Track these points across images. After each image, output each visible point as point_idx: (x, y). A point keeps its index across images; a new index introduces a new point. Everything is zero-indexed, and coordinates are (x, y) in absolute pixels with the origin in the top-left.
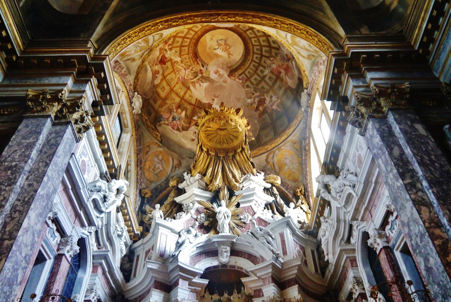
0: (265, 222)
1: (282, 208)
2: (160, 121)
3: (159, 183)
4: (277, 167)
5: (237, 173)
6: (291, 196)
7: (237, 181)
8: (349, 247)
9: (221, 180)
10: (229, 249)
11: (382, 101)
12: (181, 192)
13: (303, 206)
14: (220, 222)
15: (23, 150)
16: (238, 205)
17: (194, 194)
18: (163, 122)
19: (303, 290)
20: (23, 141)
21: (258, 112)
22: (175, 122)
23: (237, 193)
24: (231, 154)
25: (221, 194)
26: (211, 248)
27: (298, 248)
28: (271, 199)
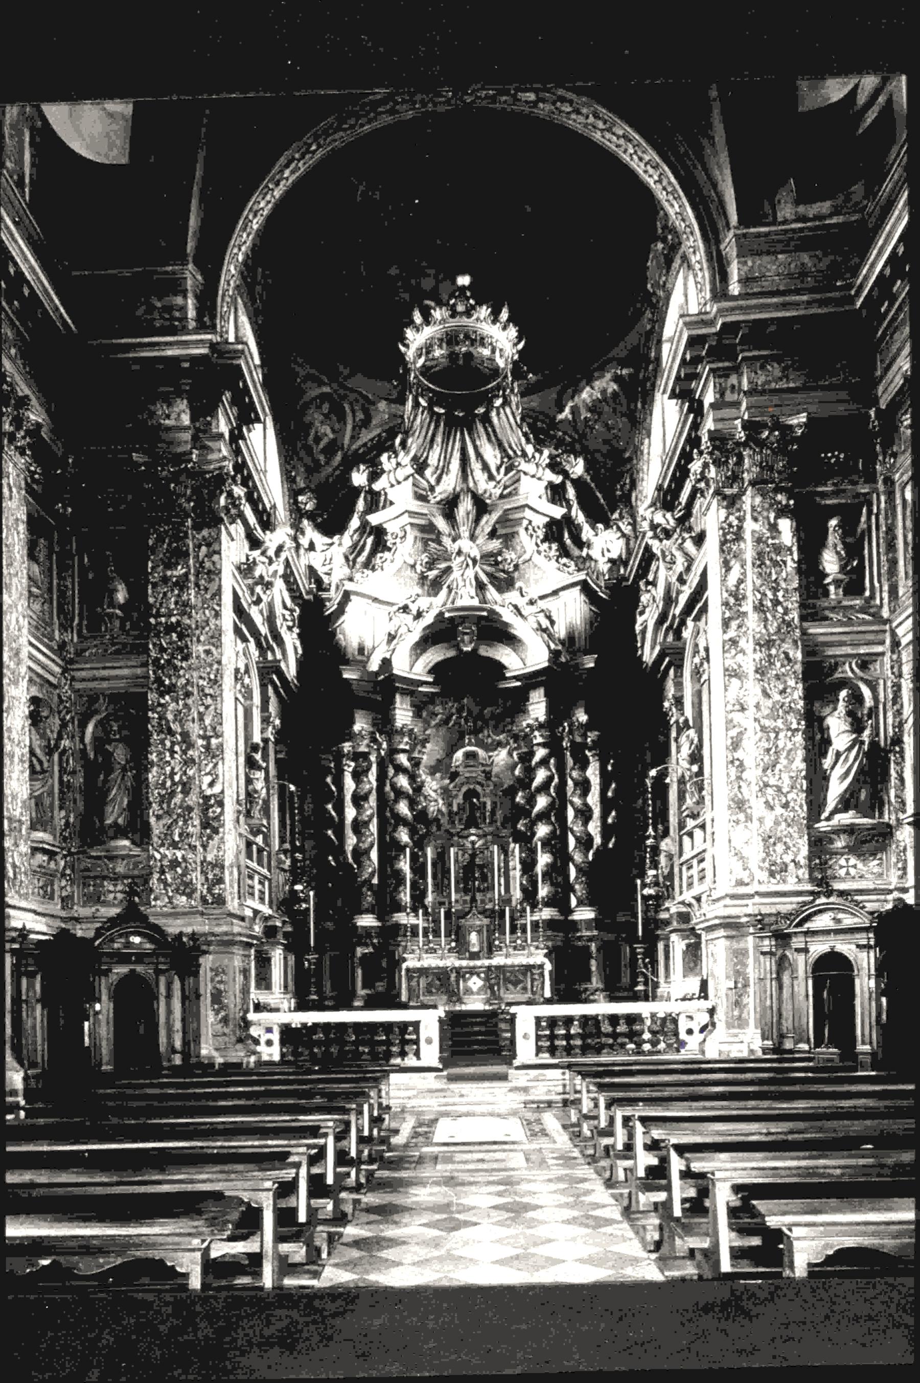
15: (176, 592)
20: (169, 573)
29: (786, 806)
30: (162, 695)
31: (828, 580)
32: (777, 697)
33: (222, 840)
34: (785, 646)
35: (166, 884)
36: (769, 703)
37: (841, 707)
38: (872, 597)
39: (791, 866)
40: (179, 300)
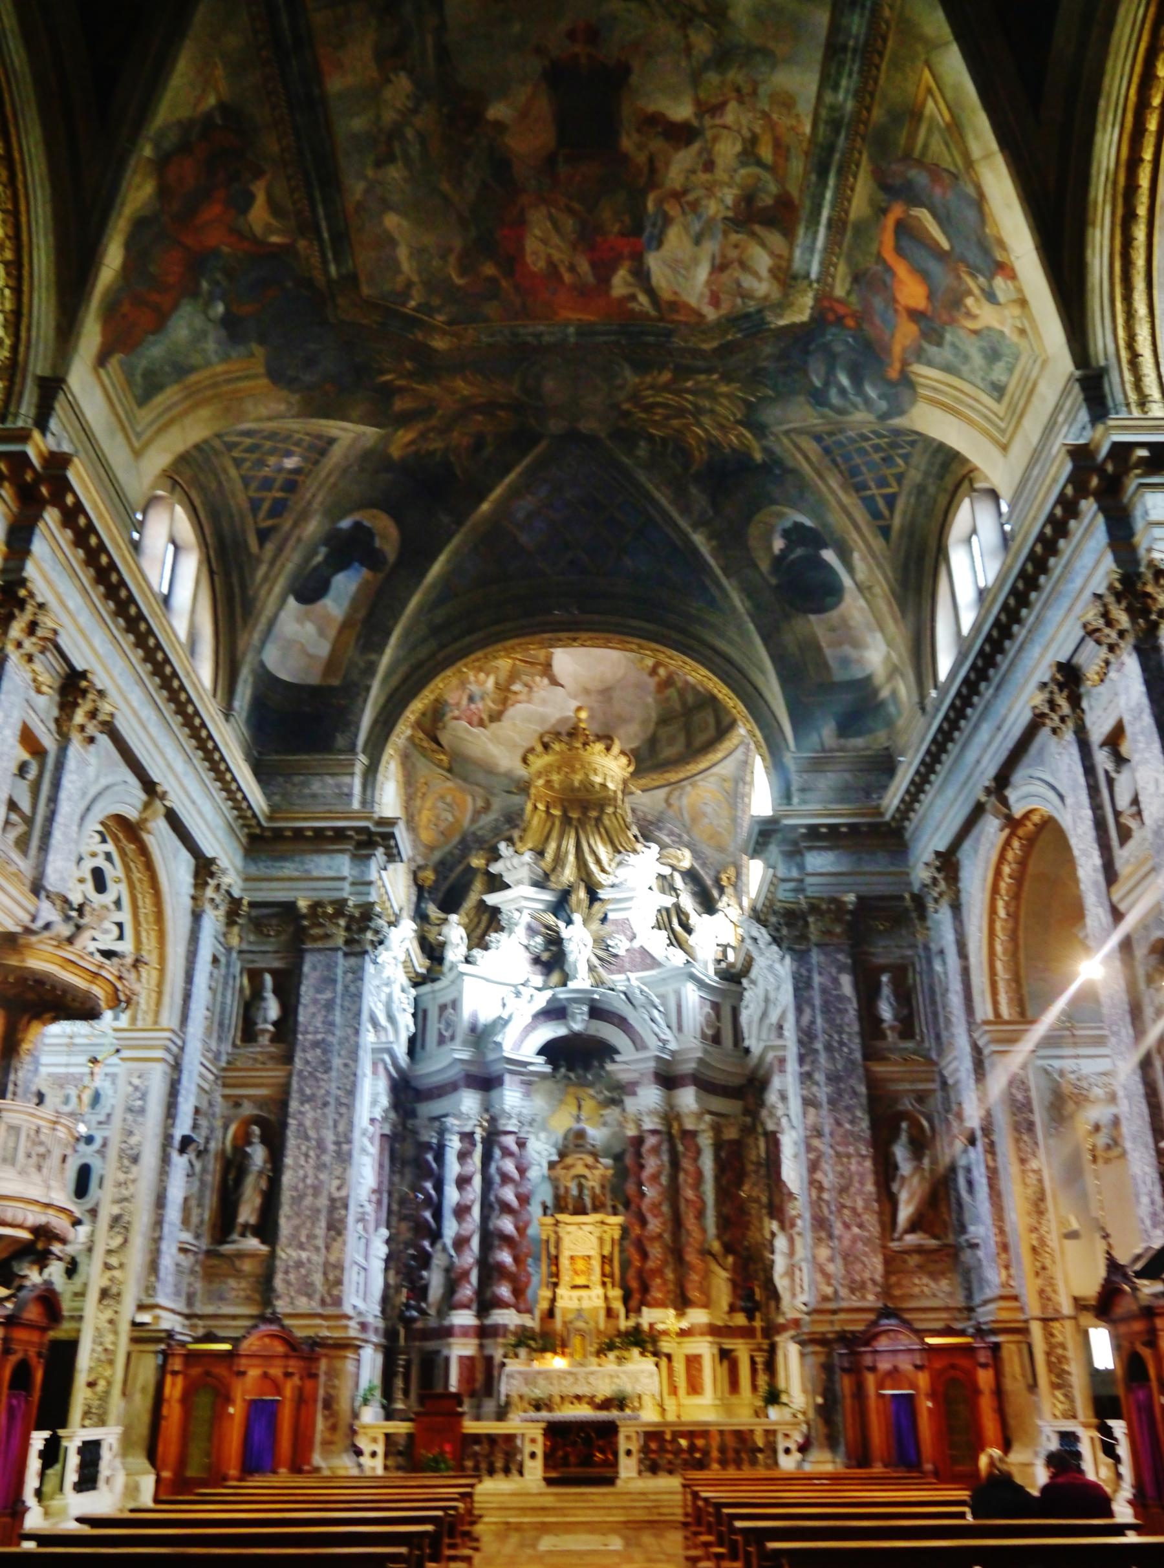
0: (653, 958)
1: (687, 916)
2: (444, 715)
3: (447, 849)
4: (686, 816)
5: (603, 851)
6: (709, 882)
7: (603, 870)
8: (780, 1042)
9: (575, 870)
10: (585, 1008)
11: (811, 919)
12: (497, 883)
13: (727, 910)
14: (571, 958)
16: (604, 920)
17: (521, 901)
18: (449, 715)
19: (705, 1085)
21: (656, 679)
22: (473, 706)
23: (602, 894)
24: (594, 814)
25: (573, 899)
26: (556, 1005)
27: (708, 1009)
28: (668, 901)
29: (861, 1226)
30: (302, 1103)
31: (885, 1025)
32: (848, 1126)
33: (344, 1243)
34: (853, 1082)
35: (288, 1283)
36: (840, 1131)
37: (904, 1137)
38: (922, 1041)
39: (869, 1285)
40: (347, 779)
